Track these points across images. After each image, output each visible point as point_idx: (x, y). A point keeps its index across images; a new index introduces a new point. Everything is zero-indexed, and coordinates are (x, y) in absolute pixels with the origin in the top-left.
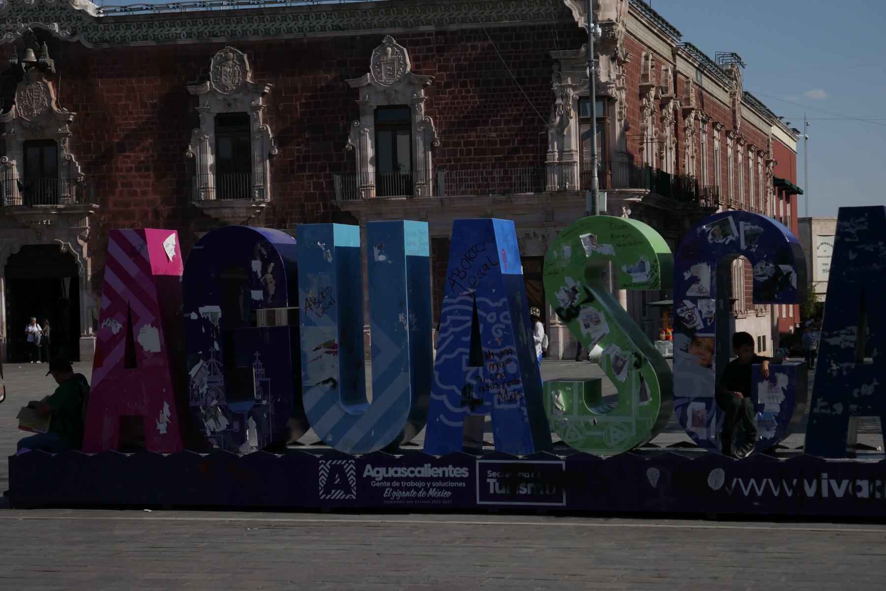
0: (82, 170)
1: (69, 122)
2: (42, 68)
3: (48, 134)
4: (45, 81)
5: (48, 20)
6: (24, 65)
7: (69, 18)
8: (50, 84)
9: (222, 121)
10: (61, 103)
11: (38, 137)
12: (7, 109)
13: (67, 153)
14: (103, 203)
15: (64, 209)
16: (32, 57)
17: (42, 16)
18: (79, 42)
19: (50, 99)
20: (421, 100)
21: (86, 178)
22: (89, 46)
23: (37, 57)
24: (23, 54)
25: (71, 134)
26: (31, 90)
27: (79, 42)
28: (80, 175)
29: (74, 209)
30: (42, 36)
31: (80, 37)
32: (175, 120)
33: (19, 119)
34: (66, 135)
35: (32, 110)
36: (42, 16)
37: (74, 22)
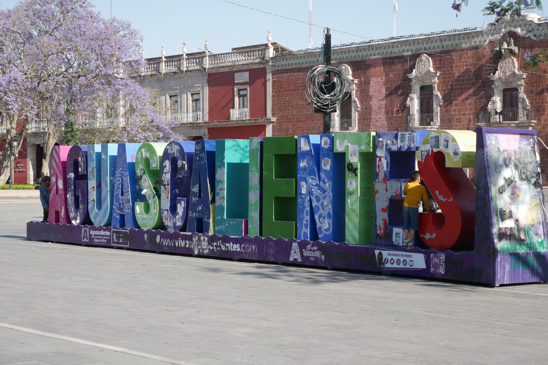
0: (529, 103)
1: (524, 78)
2: (511, 52)
3: (513, 85)
4: (513, 58)
5: (515, 27)
6: (503, 51)
7: (525, 25)
8: (515, 60)
9: (422, 88)
10: (520, 68)
11: (509, 87)
12: (494, 73)
13: (522, 94)
14: (539, 120)
15: (519, 123)
16: (505, 46)
17: (513, 25)
18: (529, 37)
19: (514, 67)
20: (435, 83)
21: (531, 107)
22: (534, 38)
23: (508, 46)
24: (501, 44)
25: (524, 84)
26: (506, 63)
27: (529, 37)
28: (528, 106)
29: (524, 123)
30: (512, 34)
31: (531, 35)
32: (400, 89)
33: (500, 78)
34: (522, 85)
35: (506, 73)
36: (513, 25)
37: (528, 26)
